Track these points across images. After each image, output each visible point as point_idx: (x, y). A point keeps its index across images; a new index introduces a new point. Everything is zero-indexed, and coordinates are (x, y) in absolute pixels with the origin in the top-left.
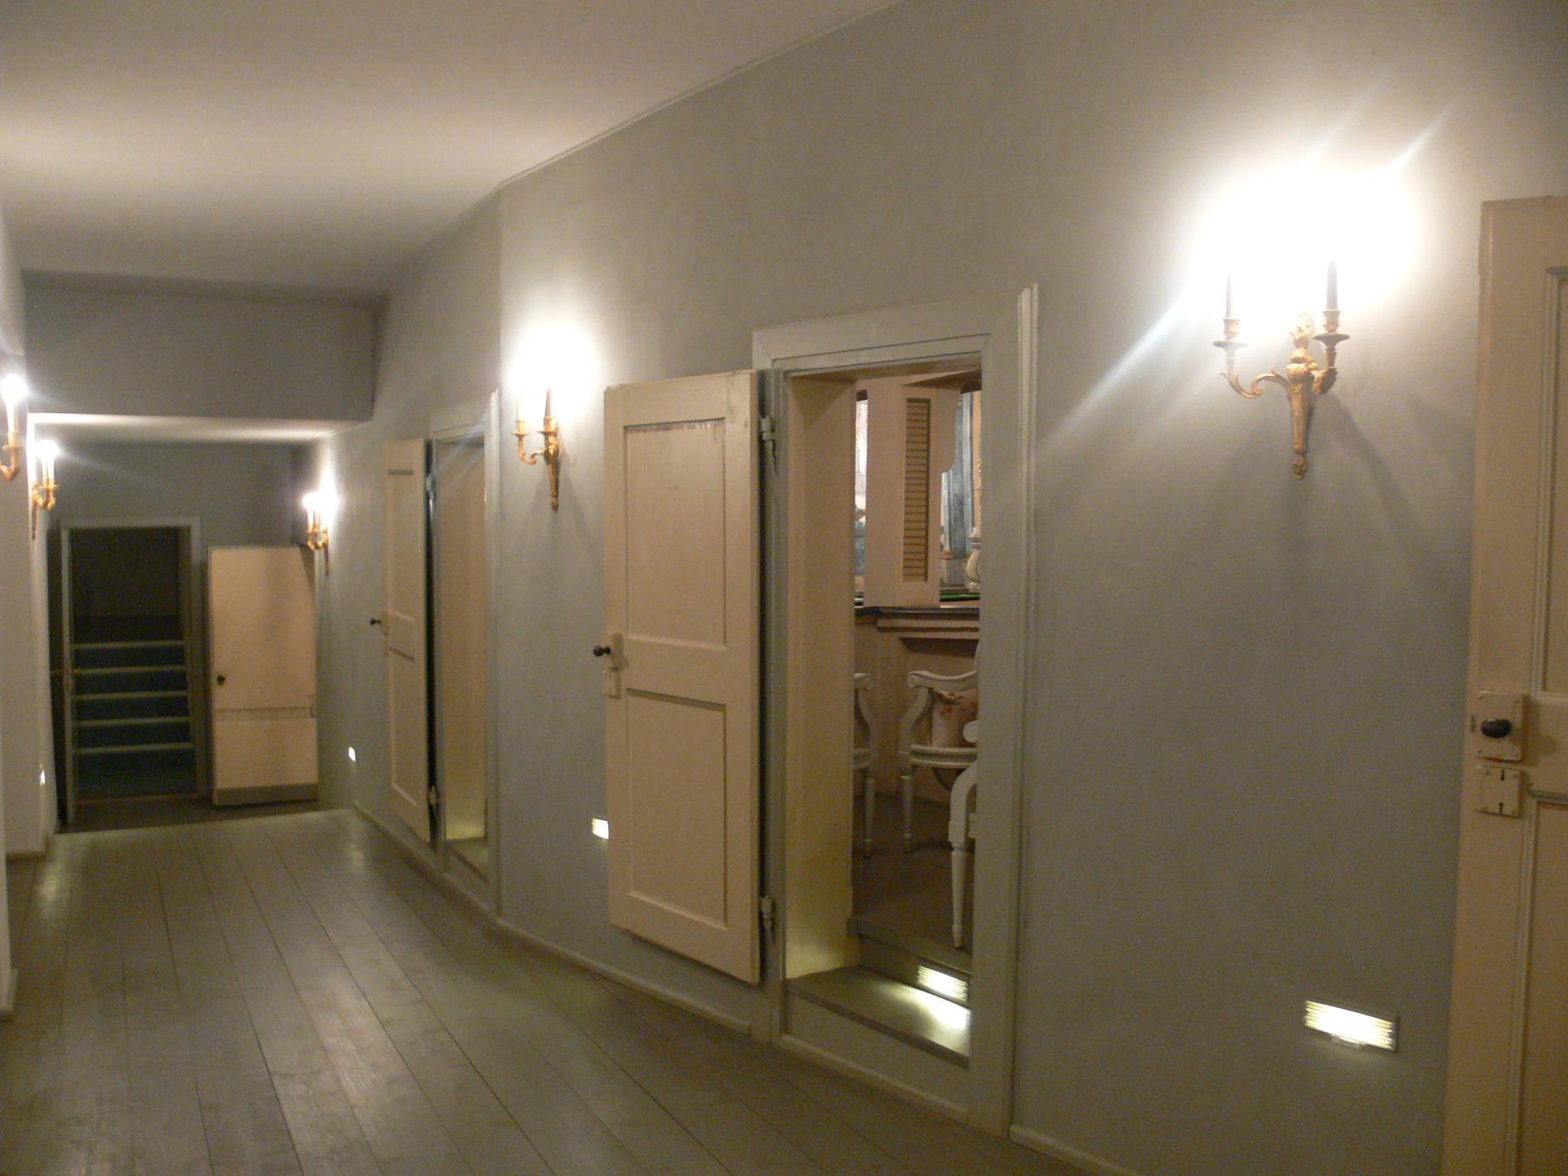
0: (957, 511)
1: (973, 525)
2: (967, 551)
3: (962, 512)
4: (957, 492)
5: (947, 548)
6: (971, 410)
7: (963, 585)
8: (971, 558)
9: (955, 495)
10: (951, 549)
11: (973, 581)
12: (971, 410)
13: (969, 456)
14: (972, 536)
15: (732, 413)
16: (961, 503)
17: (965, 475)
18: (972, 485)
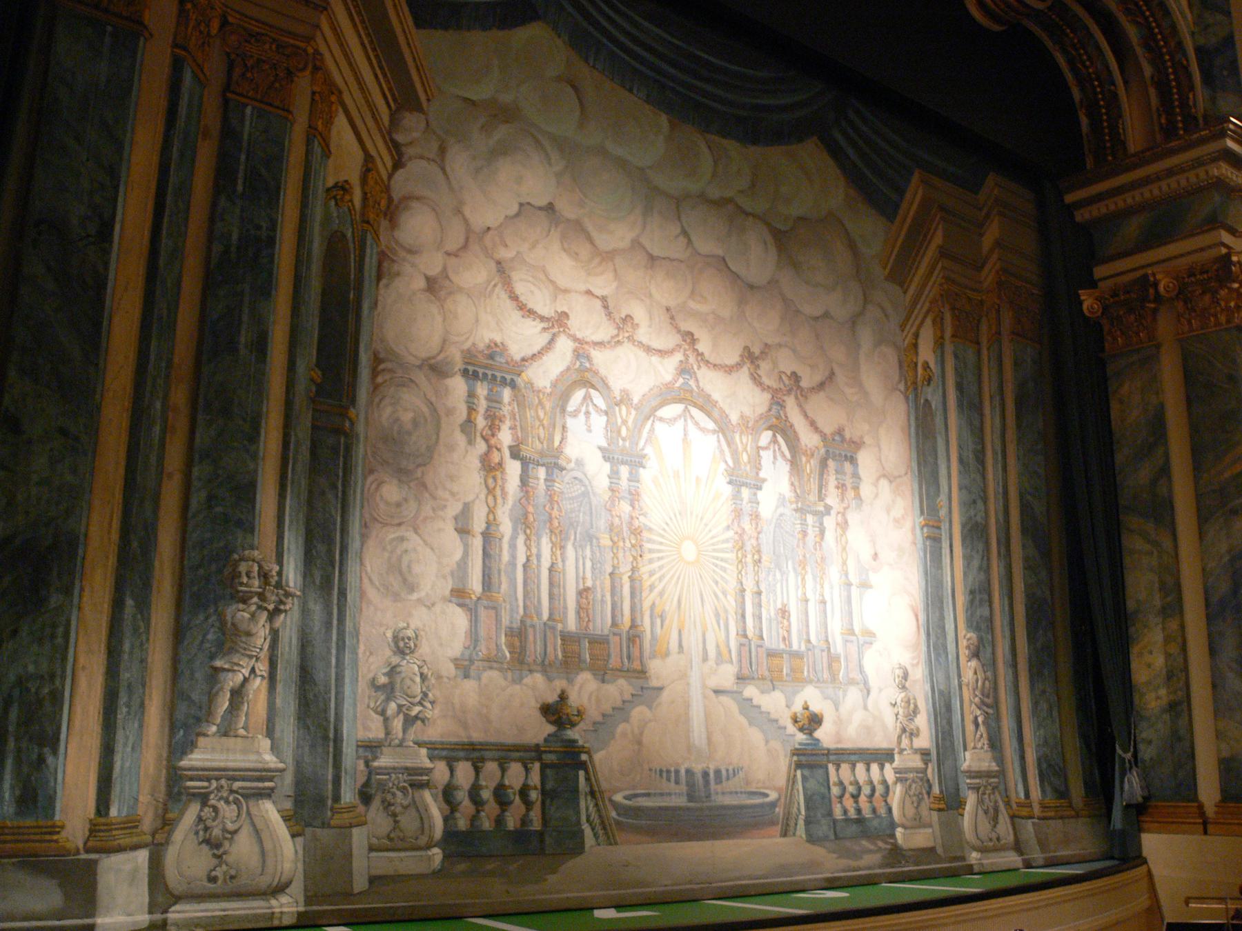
0: (944, 722)
1: (965, 749)
2: (962, 795)
3: (950, 723)
4: (942, 687)
5: (936, 790)
6: (951, 551)
7: (963, 858)
8: (968, 807)
9: (941, 693)
10: (941, 792)
11: (975, 849)
12: (951, 551)
13: (953, 626)
14: (965, 766)
15: (526, 515)
16: (949, 708)
17: (950, 657)
18: (959, 676)
